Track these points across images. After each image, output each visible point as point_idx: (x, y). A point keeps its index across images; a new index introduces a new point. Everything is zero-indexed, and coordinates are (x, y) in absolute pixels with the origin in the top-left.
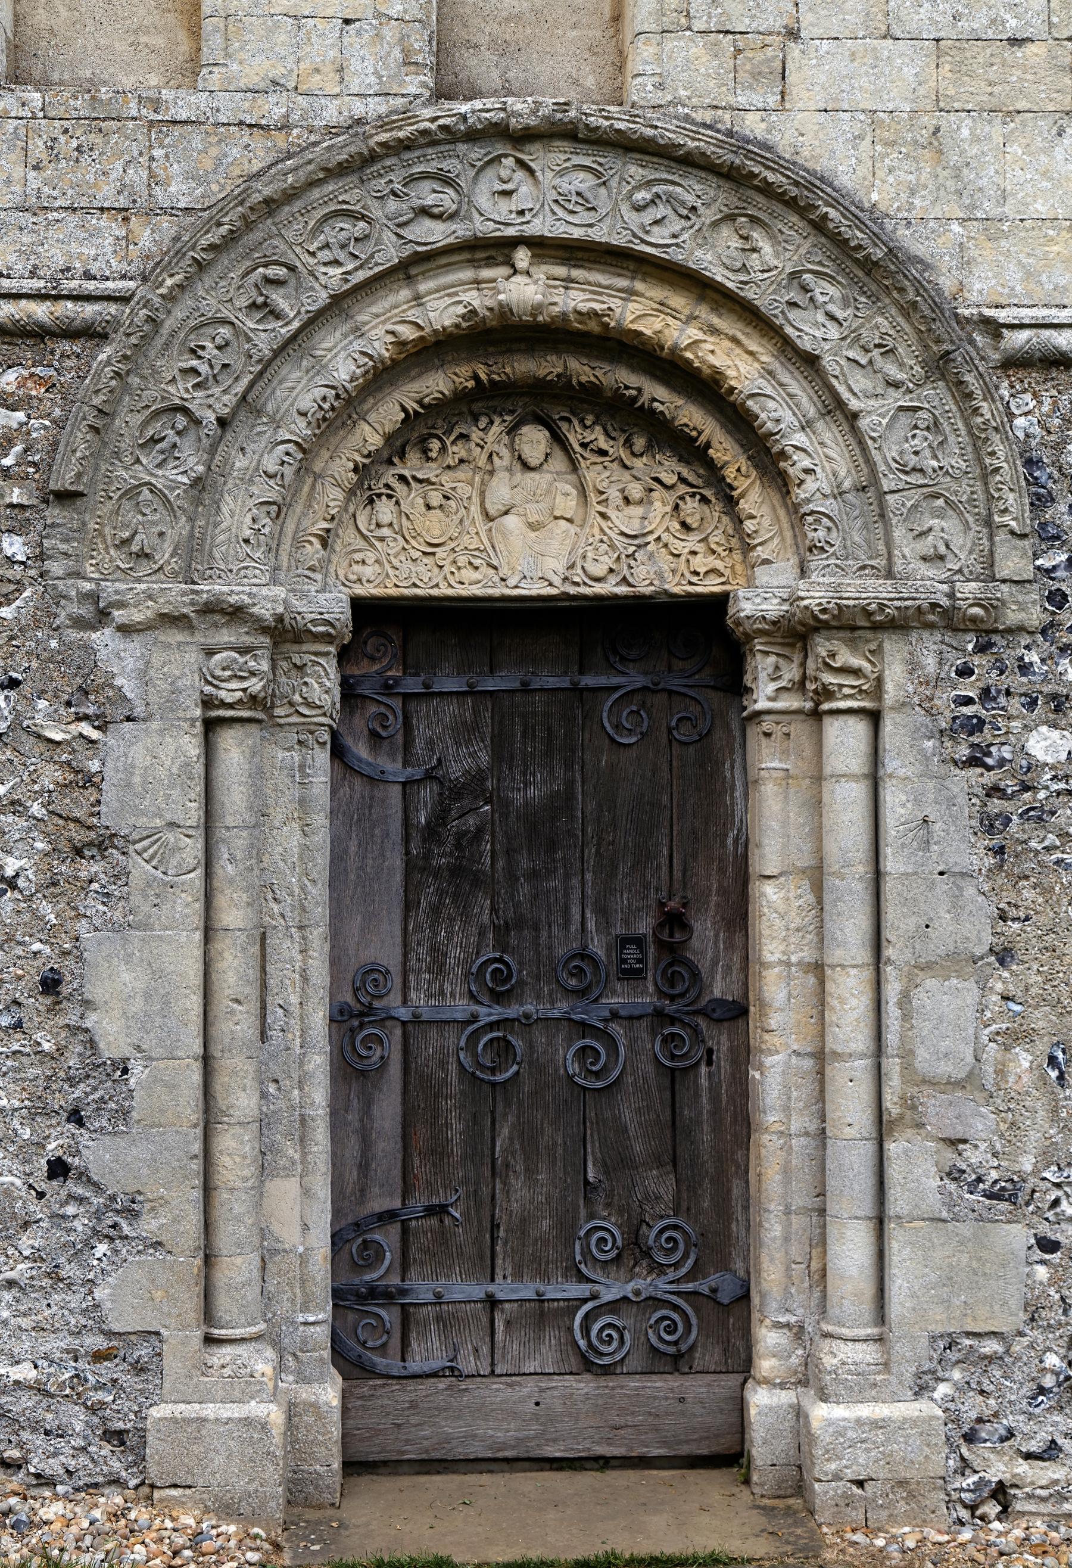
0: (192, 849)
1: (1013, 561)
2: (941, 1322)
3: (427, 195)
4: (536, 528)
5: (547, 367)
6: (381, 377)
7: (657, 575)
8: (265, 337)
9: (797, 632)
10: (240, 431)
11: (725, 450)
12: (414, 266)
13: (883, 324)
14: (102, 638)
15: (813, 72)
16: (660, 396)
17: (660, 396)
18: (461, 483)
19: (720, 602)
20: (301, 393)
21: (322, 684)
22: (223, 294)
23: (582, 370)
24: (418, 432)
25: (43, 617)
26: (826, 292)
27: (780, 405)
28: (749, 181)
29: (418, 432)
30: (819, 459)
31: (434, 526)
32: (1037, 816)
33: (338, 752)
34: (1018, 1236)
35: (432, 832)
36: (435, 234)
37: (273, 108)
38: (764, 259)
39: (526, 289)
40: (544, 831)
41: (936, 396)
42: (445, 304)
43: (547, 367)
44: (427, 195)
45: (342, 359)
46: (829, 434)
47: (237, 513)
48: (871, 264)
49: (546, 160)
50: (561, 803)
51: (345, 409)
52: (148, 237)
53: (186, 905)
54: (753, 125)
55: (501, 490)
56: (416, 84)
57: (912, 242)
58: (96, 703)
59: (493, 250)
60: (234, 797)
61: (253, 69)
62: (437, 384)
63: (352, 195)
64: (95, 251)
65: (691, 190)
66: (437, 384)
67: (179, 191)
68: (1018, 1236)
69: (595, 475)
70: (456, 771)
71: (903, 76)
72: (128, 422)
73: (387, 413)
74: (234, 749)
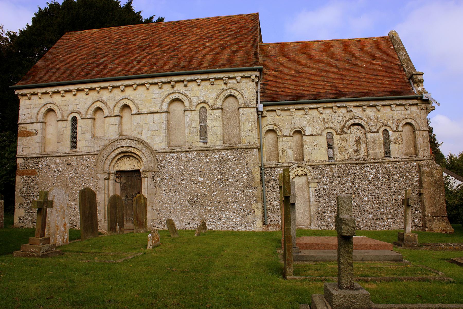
0: (103, 188)
1: (156, 167)
2: (151, 219)
3: (118, 143)
4: (128, 165)
5: (128, 154)
6: (116, 156)
7: (135, 169)
8: (108, 154)
9: (143, 172)
10: (107, 160)
11: (139, 159)
12: (117, 148)
13: (148, 151)
14: (98, 174)
15: (143, 134)
16: (135, 156)
17: (135, 156)
18: (123, 162)
19: (139, 170)
20: (111, 157)
21: (112, 177)
22: (105, 151)
23: (130, 154)
24: (119, 159)
25: (94, 173)
26: (144, 148)
27: (142, 156)
28: (139, 141)
29: (119, 159)
30: (144, 160)
31: (121, 165)
32: (158, 184)
33: (116, 181)
34: (157, 213)
35: (122, 187)
36: (119, 146)
37: (109, 138)
38: (139, 146)
39: (125, 149)
40: (130, 186)
41: (151, 156)
42: (120, 150)
43: (128, 154)
44: (118, 143)
45: (113, 155)
46: (145, 158)
47: (107, 166)
48: (147, 146)
49: (126, 140)
50: (131, 184)
51: (114, 158)
52: (101, 148)
53: (103, 192)
54: (140, 137)
55: (126, 163)
56: (118, 136)
57: (150, 145)
58: (97, 179)
59: (123, 147)
60: (106, 185)
61: (107, 136)
62: (120, 156)
63: (113, 144)
64: (97, 149)
65: (136, 142)
66: (120, 156)
67: (103, 144)
68: (157, 213)
69: (132, 161)
70: (124, 182)
71: (149, 133)
72: (99, 160)
73: (117, 158)
74: (106, 181)
